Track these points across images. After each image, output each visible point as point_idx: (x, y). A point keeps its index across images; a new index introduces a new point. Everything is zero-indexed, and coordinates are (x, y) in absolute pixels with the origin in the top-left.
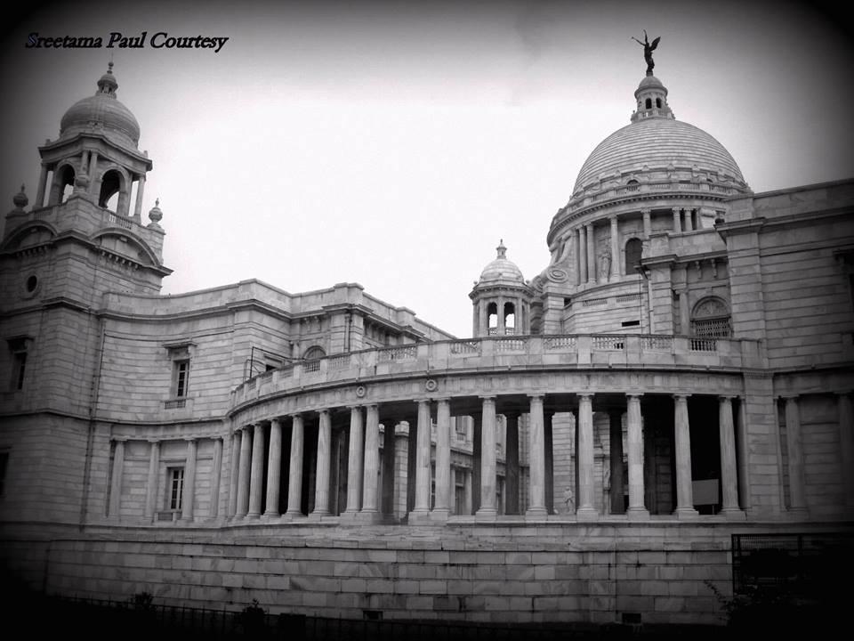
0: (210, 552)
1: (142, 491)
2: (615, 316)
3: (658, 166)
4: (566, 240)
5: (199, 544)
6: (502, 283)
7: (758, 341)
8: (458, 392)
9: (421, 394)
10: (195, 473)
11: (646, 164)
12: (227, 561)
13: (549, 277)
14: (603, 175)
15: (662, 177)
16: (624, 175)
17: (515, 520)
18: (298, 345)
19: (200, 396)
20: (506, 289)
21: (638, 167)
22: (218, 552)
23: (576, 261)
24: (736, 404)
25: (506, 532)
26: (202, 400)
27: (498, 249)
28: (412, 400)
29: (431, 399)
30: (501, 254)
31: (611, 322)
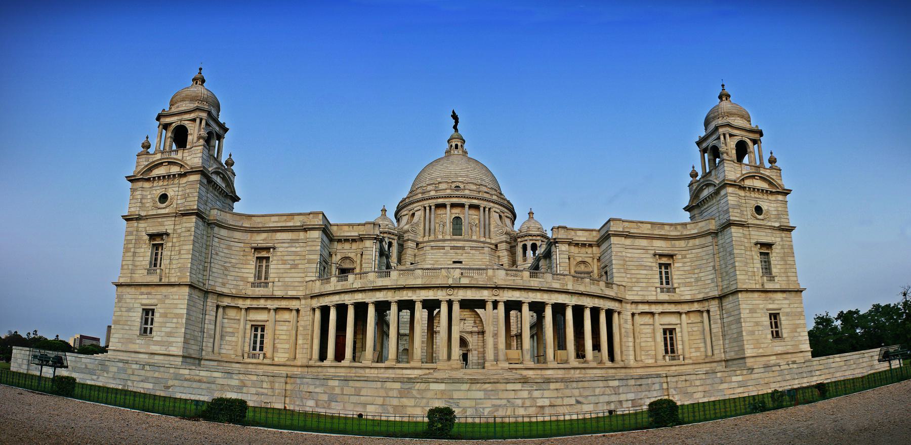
0: (527, 387)
1: (234, 339)
2: (449, 257)
4: (416, 211)
7: (625, 287)
11: (465, 179)
12: (539, 391)
14: (439, 180)
15: (474, 187)
17: (544, 366)
18: (336, 255)
19: (279, 281)
21: (460, 179)
22: (533, 387)
23: (422, 224)
24: (619, 313)
25: (539, 372)
26: (280, 284)
28: (484, 300)
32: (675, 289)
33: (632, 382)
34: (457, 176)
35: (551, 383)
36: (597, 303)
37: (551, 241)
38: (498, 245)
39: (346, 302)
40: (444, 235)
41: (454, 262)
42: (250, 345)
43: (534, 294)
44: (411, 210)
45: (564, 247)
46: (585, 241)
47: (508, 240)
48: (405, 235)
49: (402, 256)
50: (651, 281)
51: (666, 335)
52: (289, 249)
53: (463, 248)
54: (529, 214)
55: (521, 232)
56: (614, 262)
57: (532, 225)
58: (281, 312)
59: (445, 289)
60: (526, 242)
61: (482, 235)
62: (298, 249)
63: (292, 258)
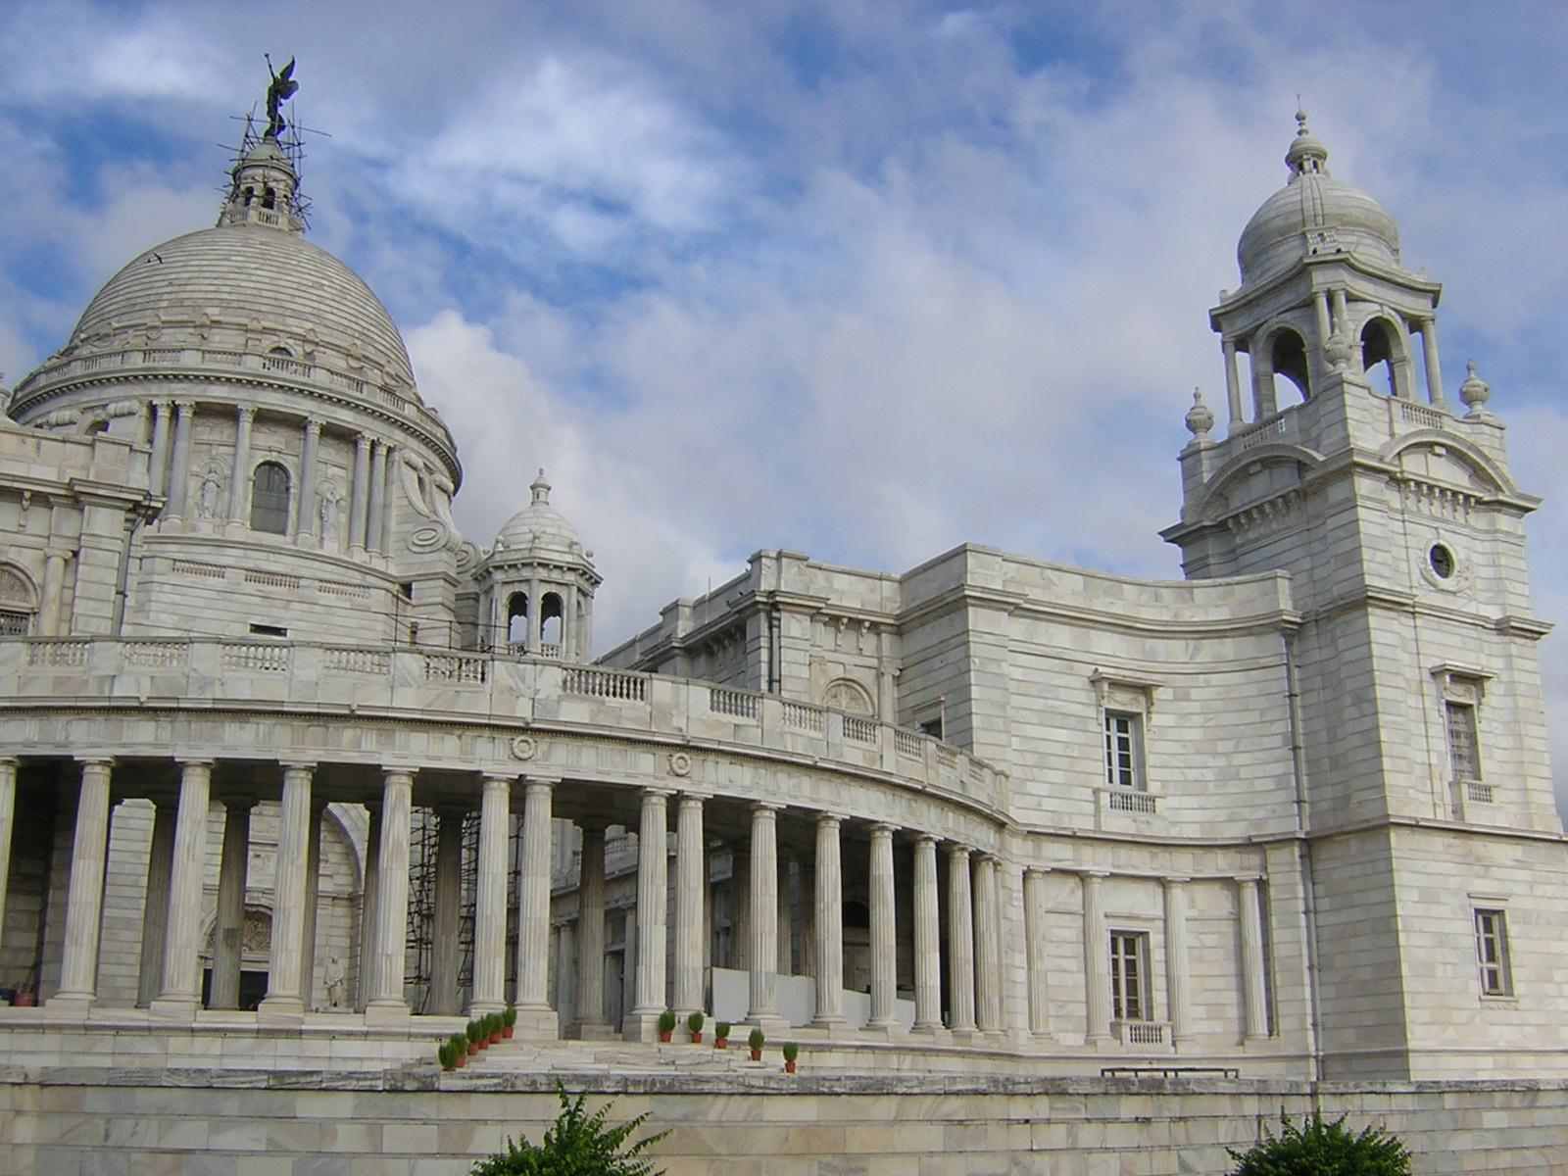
0: (1063, 1108)
2: (236, 607)
3: (338, 343)
9: (656, 778)
11: (310, 326)
14: (214, 313)
16: (273, 331)
22: (1078, 1110)
37: (758, 598)
38: (414, 586)
39: (78, 755)
43: (793, 781)
44: (92, 408)
46: (860, 611)
47: (453, 573)
53: (292, 580)
56: (975, 692)
57: (549, 530)
59: (506, 736)
60: (523, 588)
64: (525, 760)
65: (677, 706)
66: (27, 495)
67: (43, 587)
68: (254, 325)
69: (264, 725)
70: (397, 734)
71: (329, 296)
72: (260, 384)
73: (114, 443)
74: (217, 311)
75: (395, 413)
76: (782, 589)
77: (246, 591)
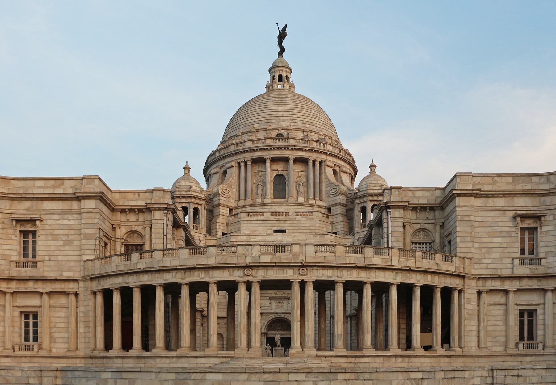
0: (312, 377)
2: (268, 225)
4: (228, 168)
5: (303, 373)
6: (194, 194)
8: (321, 277)
10: (50, 317)
11: (289, 124)
12: (325, 382)
13: (220, 193)
14: (257, 126)
15: (300, 135)
16: (275, 129)
18: (120, 228)
19: (50, 260)
20: (179, 197)
21: (283, 124)
22: (318, 377)
26: (52, 263)
27: (184, 168)
29: (303, 280)
30: (187, 172)
31: (266, 228)
32: (540, 259)
33: (442, 375)
34: (279, 120)
35: (339, 374)
36: (430, 280)
37: (382, 205)
40: (263, 197)
41: (276, 231)
42: (21, 336)
45: (397, 213)
46: (424, 203)
47: (344, 202)
48: (214, 199)
49: (212, 225)
50: (507, 250)
51: (523, 317)
52: (61, 222)
53: (286, 213)
54: (369, 167)
55: (359, 191)
56: (458, 229)
58: (56, 296)
59: (243, 269)
60: (365, 204)
61: (311, 196)
62: (72, 222)
63: (66, 232)
64: (249, 275)
65: (302, 253)
66: (136, 210)
67: (145, 236)
68: (269, 128)
69: (174, 273)
70: (210, 271)
71: (296, 111)
72: (271, 148)
73: (158, 190)
74: (257, 125)
75: (320, 149)
76: (392, 201)
77: (271, 219)
